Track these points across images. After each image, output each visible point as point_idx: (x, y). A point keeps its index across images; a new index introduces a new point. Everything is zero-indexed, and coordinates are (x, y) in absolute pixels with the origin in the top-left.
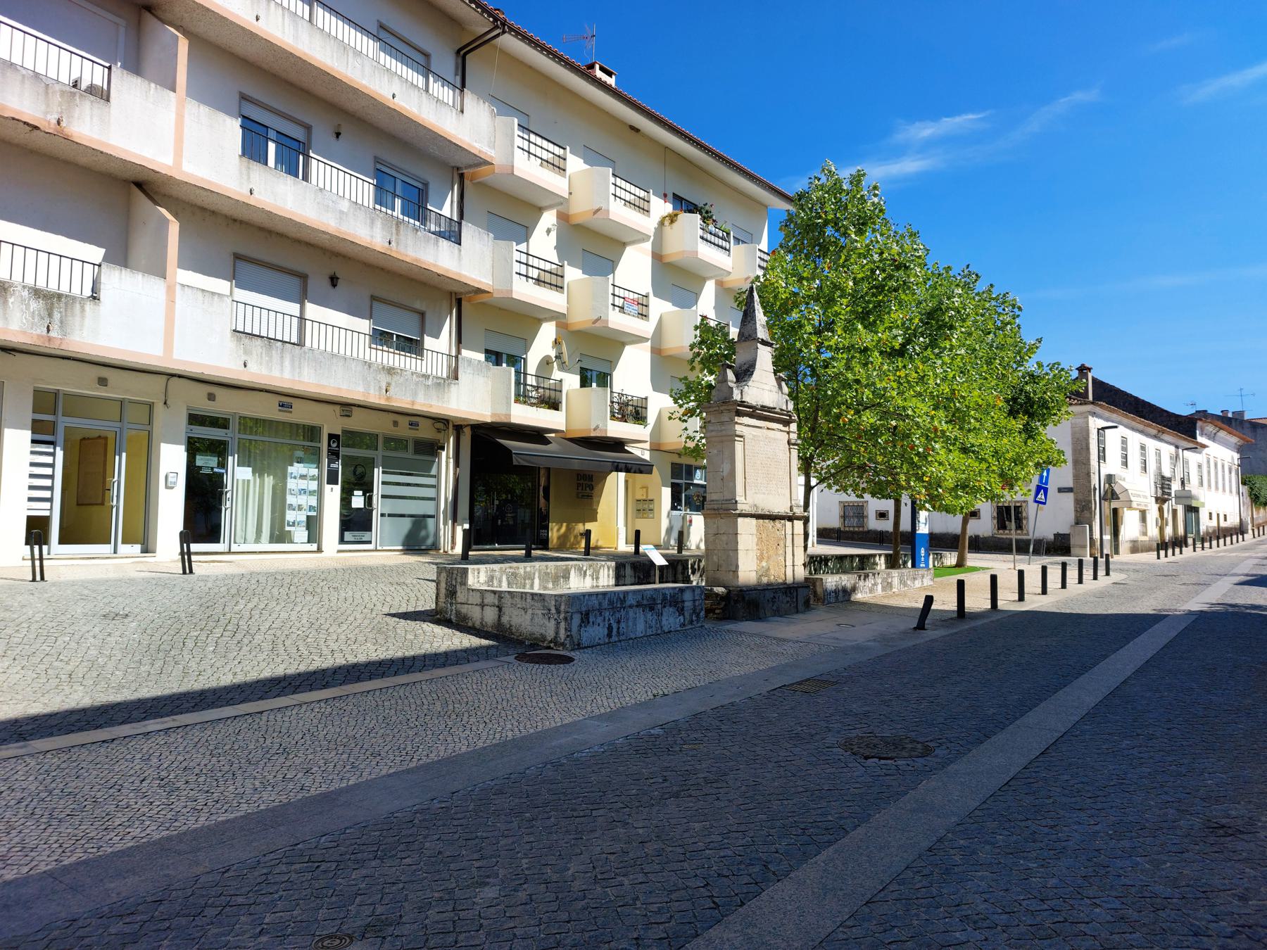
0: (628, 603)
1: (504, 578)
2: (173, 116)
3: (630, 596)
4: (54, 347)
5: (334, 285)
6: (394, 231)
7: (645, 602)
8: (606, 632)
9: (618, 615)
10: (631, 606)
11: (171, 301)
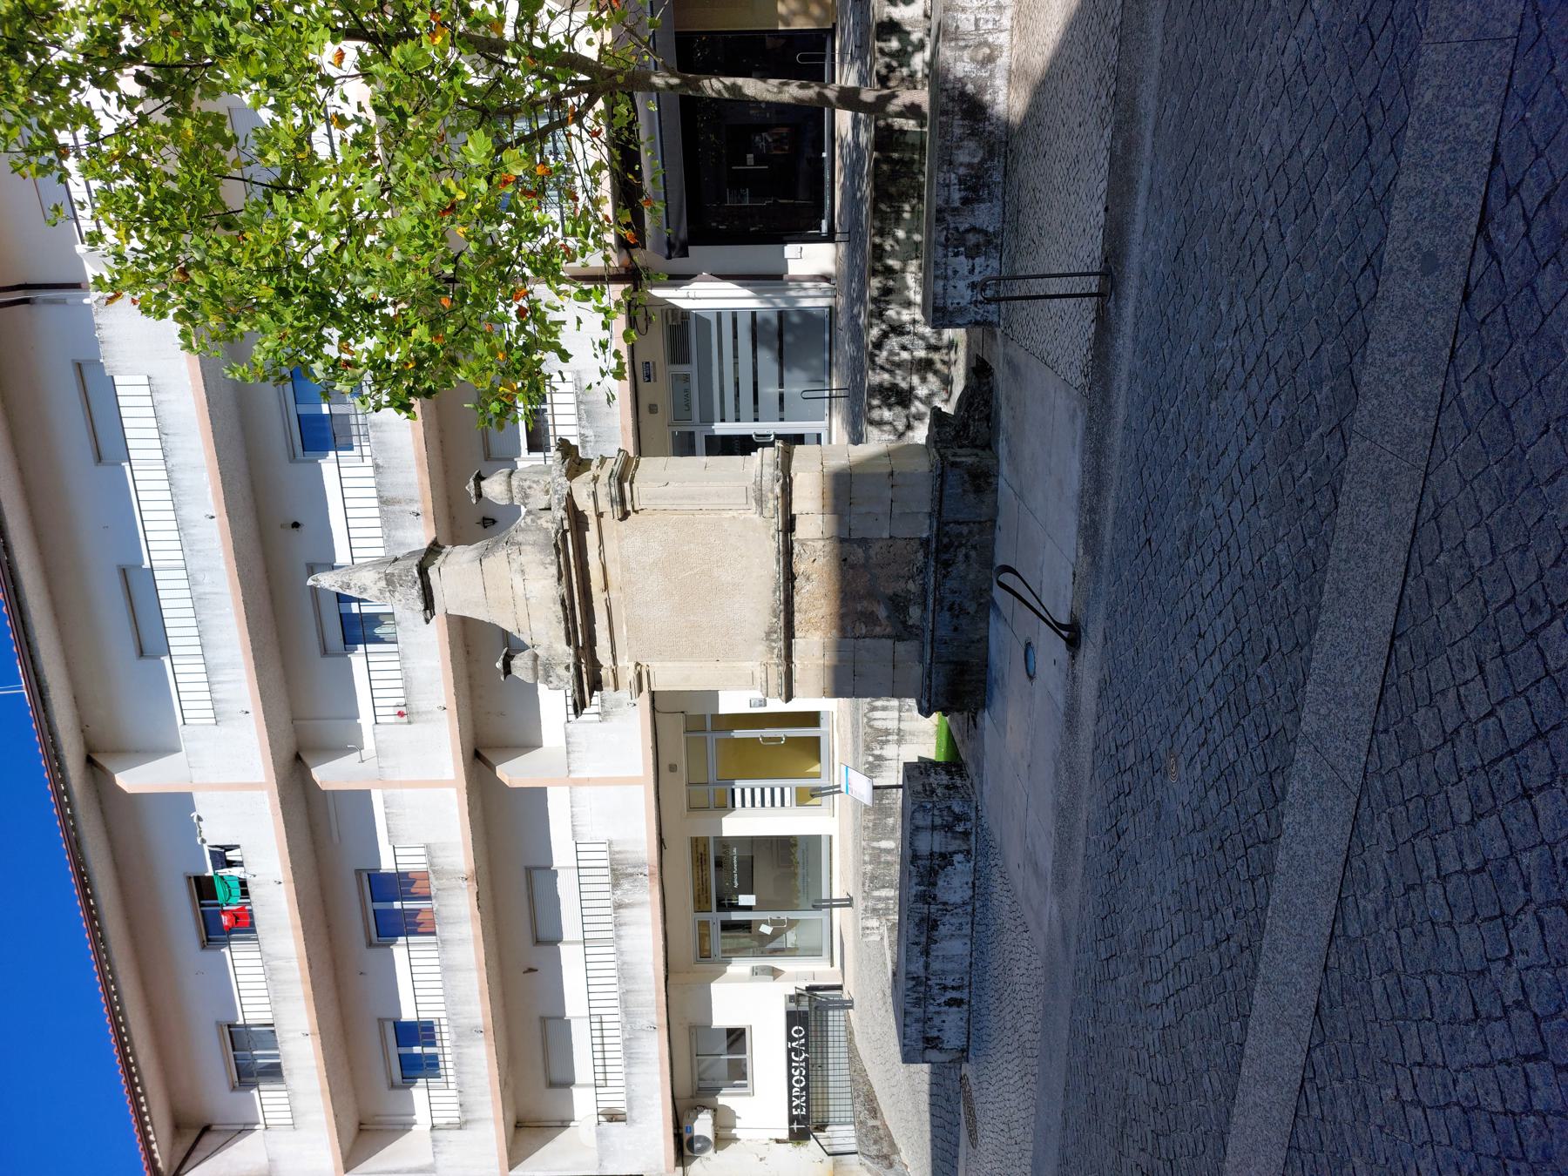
0: (922, 973)
1: (876, 893)
2: (406, 791)
3: (912, 968)
4: (656, 870)
5: (494, 522)
6: (397, 508)
7: (923, 939)
8: (955, 1009)
9: (935, 990)
10: (927, 967)
11: (588, 781)
